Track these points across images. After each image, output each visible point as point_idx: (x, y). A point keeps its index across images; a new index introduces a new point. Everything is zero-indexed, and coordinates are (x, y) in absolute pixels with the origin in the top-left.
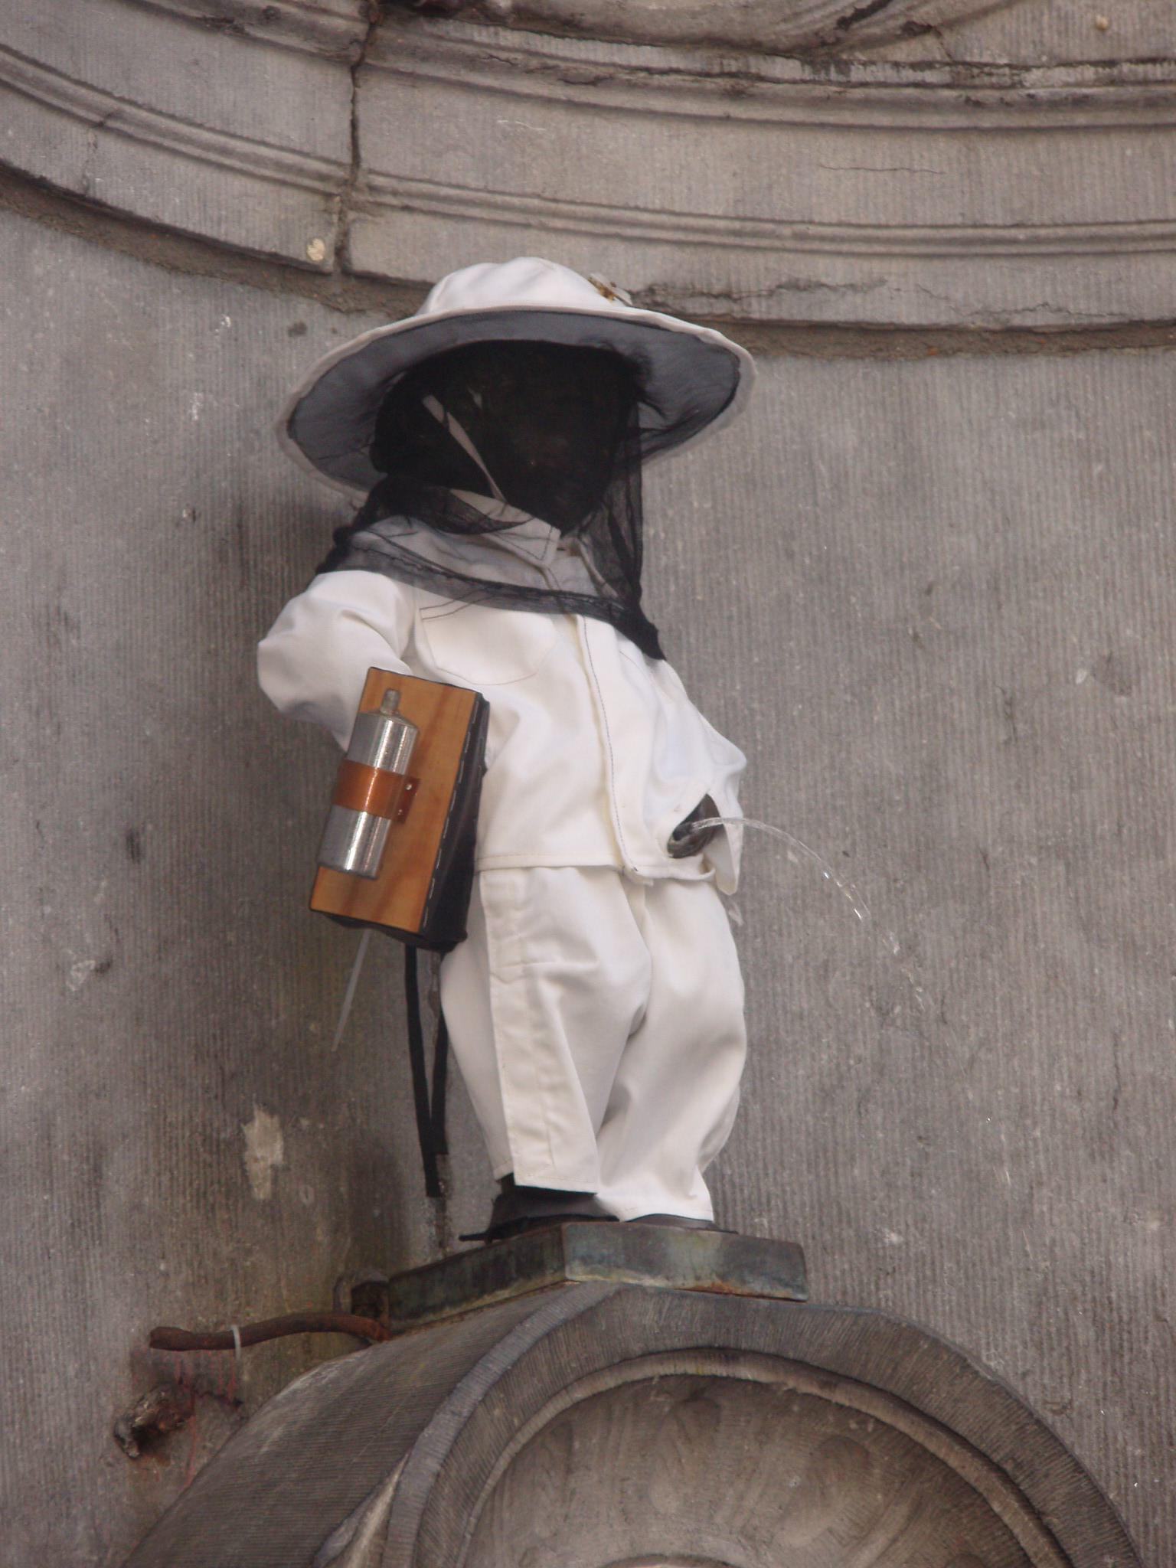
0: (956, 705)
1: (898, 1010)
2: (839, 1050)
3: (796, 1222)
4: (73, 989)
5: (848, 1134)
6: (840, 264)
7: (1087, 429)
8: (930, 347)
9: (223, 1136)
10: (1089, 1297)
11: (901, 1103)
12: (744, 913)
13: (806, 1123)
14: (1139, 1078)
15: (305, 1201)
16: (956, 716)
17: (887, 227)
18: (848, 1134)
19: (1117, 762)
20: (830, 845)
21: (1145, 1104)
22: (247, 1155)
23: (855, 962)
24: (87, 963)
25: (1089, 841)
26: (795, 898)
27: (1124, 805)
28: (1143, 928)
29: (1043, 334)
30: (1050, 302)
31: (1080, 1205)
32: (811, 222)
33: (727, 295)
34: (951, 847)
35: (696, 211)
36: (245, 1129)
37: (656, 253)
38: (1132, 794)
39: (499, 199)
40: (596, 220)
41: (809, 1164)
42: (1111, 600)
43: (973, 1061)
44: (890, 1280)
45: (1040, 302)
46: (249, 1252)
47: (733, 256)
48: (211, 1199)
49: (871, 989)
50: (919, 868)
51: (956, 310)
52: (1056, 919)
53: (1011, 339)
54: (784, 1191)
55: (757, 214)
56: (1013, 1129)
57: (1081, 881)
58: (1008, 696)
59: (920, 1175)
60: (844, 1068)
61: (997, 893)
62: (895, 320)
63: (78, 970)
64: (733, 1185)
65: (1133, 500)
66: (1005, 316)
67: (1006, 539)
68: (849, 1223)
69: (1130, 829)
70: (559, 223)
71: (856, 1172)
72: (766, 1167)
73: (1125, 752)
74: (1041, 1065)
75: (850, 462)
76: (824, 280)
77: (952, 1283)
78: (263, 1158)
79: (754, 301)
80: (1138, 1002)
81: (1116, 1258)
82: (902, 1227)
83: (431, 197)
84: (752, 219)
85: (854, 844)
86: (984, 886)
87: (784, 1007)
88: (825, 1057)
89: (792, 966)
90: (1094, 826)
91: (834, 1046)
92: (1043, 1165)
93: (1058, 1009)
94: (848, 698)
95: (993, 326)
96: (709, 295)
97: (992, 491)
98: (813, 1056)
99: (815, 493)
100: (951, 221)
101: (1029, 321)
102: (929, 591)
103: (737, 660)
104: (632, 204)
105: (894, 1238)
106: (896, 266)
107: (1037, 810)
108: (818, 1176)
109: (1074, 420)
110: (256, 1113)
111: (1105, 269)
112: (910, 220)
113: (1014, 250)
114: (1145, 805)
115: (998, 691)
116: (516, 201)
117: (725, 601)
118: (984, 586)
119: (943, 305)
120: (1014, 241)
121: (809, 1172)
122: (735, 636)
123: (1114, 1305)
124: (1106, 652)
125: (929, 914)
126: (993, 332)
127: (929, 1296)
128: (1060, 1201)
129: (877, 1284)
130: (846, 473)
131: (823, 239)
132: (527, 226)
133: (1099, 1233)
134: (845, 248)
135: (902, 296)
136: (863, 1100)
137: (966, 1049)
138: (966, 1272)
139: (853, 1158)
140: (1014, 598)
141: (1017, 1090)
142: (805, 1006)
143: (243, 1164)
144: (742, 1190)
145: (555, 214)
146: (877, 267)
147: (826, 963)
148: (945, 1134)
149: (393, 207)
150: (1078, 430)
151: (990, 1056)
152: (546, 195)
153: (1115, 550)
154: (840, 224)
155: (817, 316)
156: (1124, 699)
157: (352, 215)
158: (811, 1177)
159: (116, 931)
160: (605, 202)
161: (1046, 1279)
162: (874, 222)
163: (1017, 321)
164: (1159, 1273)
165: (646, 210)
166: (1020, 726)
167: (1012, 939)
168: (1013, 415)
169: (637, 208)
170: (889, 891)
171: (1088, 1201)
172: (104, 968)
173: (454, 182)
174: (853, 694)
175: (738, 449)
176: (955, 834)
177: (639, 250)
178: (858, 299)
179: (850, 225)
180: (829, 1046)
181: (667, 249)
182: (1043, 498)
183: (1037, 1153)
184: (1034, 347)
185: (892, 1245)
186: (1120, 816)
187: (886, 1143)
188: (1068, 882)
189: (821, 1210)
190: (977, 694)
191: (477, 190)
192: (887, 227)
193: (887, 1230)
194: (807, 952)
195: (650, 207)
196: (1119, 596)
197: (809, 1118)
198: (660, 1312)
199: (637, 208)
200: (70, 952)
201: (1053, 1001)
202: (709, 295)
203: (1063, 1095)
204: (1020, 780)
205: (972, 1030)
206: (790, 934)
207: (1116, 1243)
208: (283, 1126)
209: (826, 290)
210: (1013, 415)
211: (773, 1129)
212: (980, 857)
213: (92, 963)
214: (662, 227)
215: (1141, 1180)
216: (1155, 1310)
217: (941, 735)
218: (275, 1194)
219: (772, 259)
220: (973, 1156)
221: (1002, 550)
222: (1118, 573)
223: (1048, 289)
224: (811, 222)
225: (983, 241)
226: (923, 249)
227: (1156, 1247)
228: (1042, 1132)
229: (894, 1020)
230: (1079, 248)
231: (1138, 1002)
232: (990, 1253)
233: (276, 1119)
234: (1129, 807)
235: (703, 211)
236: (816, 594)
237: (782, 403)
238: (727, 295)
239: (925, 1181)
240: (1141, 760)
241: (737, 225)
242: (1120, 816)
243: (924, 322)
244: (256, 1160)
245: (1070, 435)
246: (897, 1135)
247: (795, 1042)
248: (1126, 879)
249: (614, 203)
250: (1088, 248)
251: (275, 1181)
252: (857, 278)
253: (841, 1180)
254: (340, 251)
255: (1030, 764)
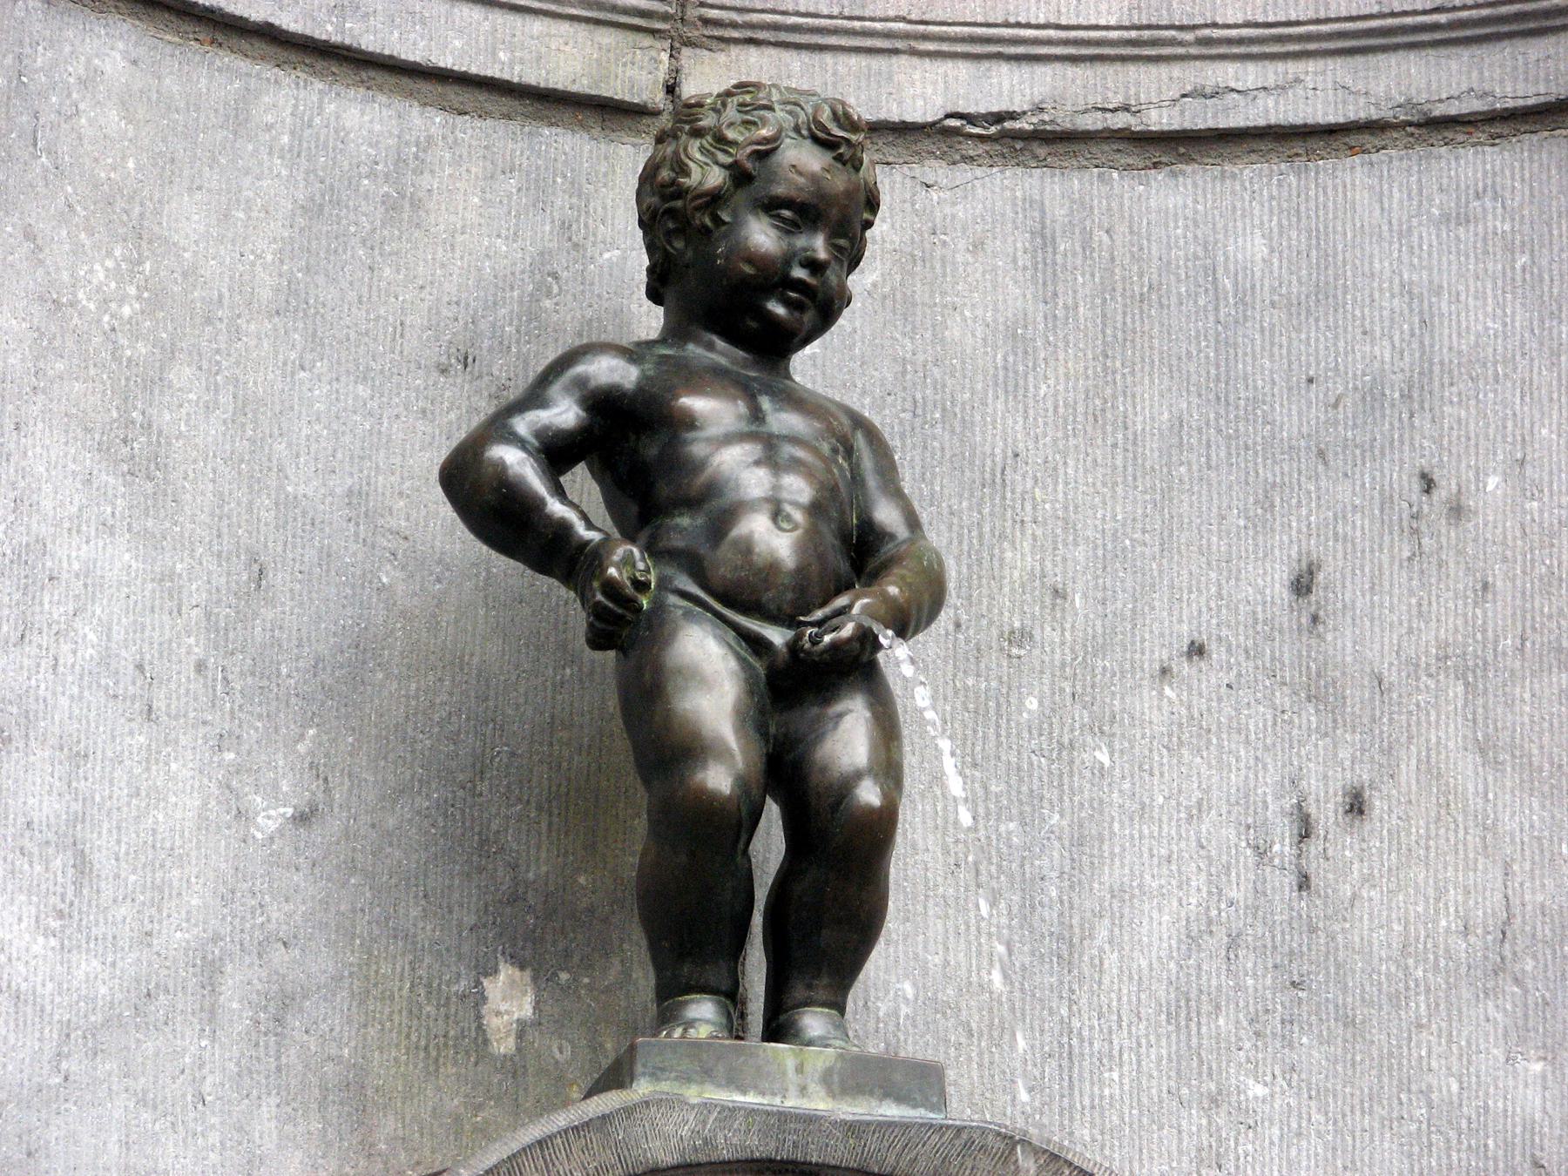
0: (1359, 523)
1: (1276, 848)
2: (1210, 893)
3: (1151, 1076)
4: (259, 836)
5: (1214, 982)
6: (1251, 67)
7: (1513, 220)
8: (1351, 148)
9: (454, 988)
10: (1464, 1147)
11: (1274, 947)
12: (1112, 754)
13: (1169, 971)
14: (1529, 908)
15: (558, 1055)
16: (1358, 533)
17: (1298, 23)
18: (1214, 982)
19: (1524, 573)
20: (1213, 680)
21: (1534, 935)
22: (485, 1010)
23: (1233, 800)
24: (282, 810)
25: (1490, 658)
26: (1170, 735)
27: (1529, 617)
28: (1542, 747)
29: (1470, 122)
30: (1475, 86)
31: (1461, 1048)
32: (1215, 25)
33: (1126, 108)
34: (1344, 674)
35: (1085, 23)
36: (486, 982)
37: (1045, 72)
38: (1537, 605)
39: (857, 24)
40: (973, 40)
41: (1169, 1014)
42: (1527, 399)
43: (1354, 897)
44: (1251, 1135)
45: (1464, 87)
46: (480, 1107)
47: (1132, 69)
48: (434, 1054)
49: (1248, 827)
50: (1309, 699)
51: (1377, 105)
52: (1451, 745)
53: (1437, 127)
54: (1139, 1045)
55: (1154, 21)
56: (1393, 969)
57: (1480, 701)
58: (1415, 509)
59: (1291, 1023)
60: (1214, 913)
61: (1391, 719)
62: (1310, 121)
63: (269, 817)
64: (1082, 1040)
65: (1555, 291)
66: (1426, 108)
67: (1422, 343)
68: (1210, 1075)
69: (1533, 643)
70: (931, 46)
71: (1221, 1022)
72: (1119, 1017)
73: (1532, 560)
74: (1427, 899)
75: (1258, 274)
76: (1233, 85)
77: (1318, 1133)
78: (507, 1012)
79: (1154, 114)
80: (1532, 826)
81: (1495, 1102)
82: (1268, 1079)
83: (776, 27)
84: (1149, 27)
85: (1239, 675)
86: (1378, 713)
87: (1151, 850)
88: (1194, 901)
89: (1162, 807)
90: (1496, 642)
91: (1205, 890)
92: (1423, 1006)
93: (1448, 840)
94: (1242, 523)
95: (1415, 119)
96: (1104, 110)
97: (1410, 292)
98: (1180, 900)
99: (1217, 309)
100: (1367, 11)
101: (1453, 109)
102: (1335, 406)
103: (1119, 489)
104: (1012, 20)
105: (1260, 1090)
106: (1311, 65)
107: (1438, 629)
108: (1178, 1027)
109: (1500, 211)
110: (501, 966)
111: (1536, 49)
112: (1322, 15)
113: (1438, 36)
114: (1550, 617)
115: (1405, 505)
116: (878, 26)
117: (1109, 428)
118: (1397, 395)
119: (1362, 101)
120: (1436, 27)
121: (1168, 1022)
122: (1119, 462)
123: (1490, 1154)
124: (1519, 456)
125: (1316, 746)
126: (1418, 125)
127: (1294, 1152)
128: (1440, 1044)
129: (1237, 1139)
130: (1253, 287)
131: (1229, 41)
132: (896, 52)
133: (1478, 1077)
134: (1255, 49)
135: (1318, 92)
136: (1234, 942)
137: (1348, 887)
138: (1335, 1123)
139: (1218, 1007)
140: (1426, 406)
141: (1401, 928)
142: (1175, 848)
143: (479, 1017)
144: (1091, 1044)
145: (925, 37)
146: (1293, 68)
147: (1199, 803)
148: (1321, 978)
149: (736, 41)
150: (1503, 221)
151: (1373, 893)
152: (913, 17)
153: (1534, 346)
154: (1247, 25)
155: (1223, 124)
156: (1535, 504)
157: (686, 52)
158: (1171, 1028)
159: (326, 779)
160: (980, 19)
161: (1419, 1129)
162: (1284, 19)
163: (1439, 111)
164: (1537, 1116)
165: (1028, 26)
166: (1426, 541)
167: (1403, 767)
168: (1435, 211)
169: (1018, 25)
170: (1275, 724)
171: (1469, 1043)
172: (303, 818)
173: (803, 10)
174: (1247, 518)
175: (1136, 268)
176: (1349, 659)
177: (1026, 70)
178: (1271, 102)
179: (1257, 25)
180: (1199, 890)
181: (1058, 66)
182: (1463, 298)
183: (1417, 994)
184: (1461, 138)
185: (1256, 1098)
186: (1524, 630)
187: (1256, 990)
188: (1466, 705)
189: (1179, 1062)
190: (1382, 511)
191: (831, 17)
192: (1298, 23)
193: (1251, 1082)
194: (1180, 791)
195: (1033, 21)
196: (1536, 394)
197: (1172, 965)
198: (704, 1122)
199: (1018, 25)
200: (259, 800)
201: (1442, 831)
202: (1104, 110)
203: (1447, 930)
204: (1421, 598)
205: (1356, 866)
206: (1162, 775)
207: (1496, 1087)
208: (535, 979)
209: (1235, 95)
210: (1435, 211)
211: (1131, 978)
212: (1376, 683)
213: (290, 811)
214: (1049, 42)
215: (1526, 1015)
216: (1533, 1155)
217: (1340, 555)
218: (519, 1049)
219: (1176, 70)
220: (1350, 1000)
221: (1417, 355)
222: (1536, 370)
223: (1475, 74)
224: (1215, 25)
225: (1404, 30)
226: (1340, 44)
227: (1539, 1089)
228: (1425, 971)
229: (1271, 860)
230: (1505, 28)
231: (1532, 826)
232: (1362, 1102)
233: (528, 973)
234: (1533, 618)
235: (1093, 22)
236: (1212, 416)
237: (1186, 218)
238: (1126, 108)
239: (1296, 1029)
240: (1549, 567)
241: (1134, 34)
242: (1524, 630)
243: (1341, 120)
244: (498, 1014)
245: (1495, 227)
246: (1269, 981)
247: (1162, 887)
248: (1527, 696)
249: (991, 21)
250: (1514, 27)
251: (520, 1035)
252: (1271, 82)
253: (1204, 1030)
254: (671, 89)
255: (1433, 580)
